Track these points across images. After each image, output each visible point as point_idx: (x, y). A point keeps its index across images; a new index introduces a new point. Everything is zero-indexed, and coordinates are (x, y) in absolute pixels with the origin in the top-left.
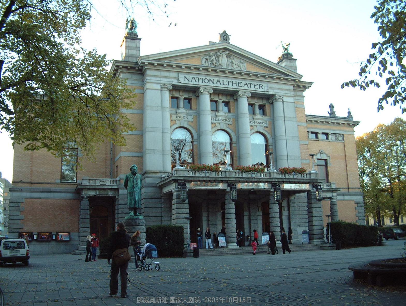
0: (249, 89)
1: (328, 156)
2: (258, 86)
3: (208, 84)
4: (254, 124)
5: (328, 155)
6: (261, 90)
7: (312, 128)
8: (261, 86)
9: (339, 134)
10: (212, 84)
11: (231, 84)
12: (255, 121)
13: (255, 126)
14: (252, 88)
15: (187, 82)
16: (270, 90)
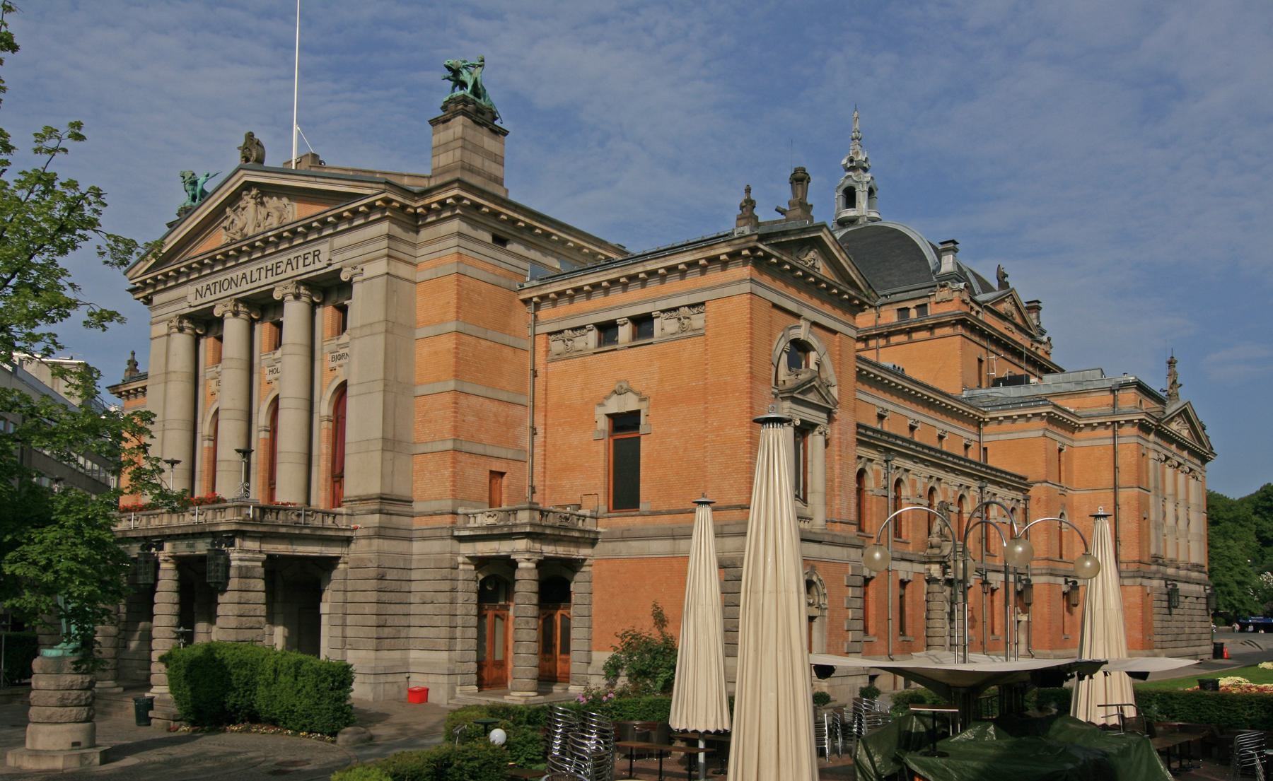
0: (295, 273)
1: (642, 400)
2: (311, 259)
3: (230, 292)
4: (339, 362)
5: (646, 393)
6: (318, 265)
7: (594, 312)
8: (316, 255)
9: (691, 306)
10: (234, 290)
11: (263, 272)
12: (341, 352)
13: (341, 366)
14: (302, 270)
15: (200, 301)
16: (336, 259)
